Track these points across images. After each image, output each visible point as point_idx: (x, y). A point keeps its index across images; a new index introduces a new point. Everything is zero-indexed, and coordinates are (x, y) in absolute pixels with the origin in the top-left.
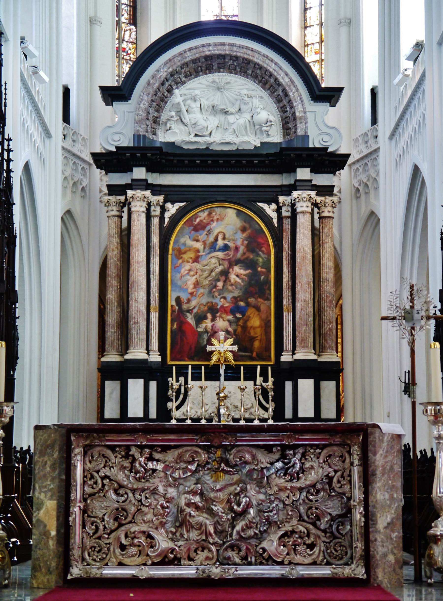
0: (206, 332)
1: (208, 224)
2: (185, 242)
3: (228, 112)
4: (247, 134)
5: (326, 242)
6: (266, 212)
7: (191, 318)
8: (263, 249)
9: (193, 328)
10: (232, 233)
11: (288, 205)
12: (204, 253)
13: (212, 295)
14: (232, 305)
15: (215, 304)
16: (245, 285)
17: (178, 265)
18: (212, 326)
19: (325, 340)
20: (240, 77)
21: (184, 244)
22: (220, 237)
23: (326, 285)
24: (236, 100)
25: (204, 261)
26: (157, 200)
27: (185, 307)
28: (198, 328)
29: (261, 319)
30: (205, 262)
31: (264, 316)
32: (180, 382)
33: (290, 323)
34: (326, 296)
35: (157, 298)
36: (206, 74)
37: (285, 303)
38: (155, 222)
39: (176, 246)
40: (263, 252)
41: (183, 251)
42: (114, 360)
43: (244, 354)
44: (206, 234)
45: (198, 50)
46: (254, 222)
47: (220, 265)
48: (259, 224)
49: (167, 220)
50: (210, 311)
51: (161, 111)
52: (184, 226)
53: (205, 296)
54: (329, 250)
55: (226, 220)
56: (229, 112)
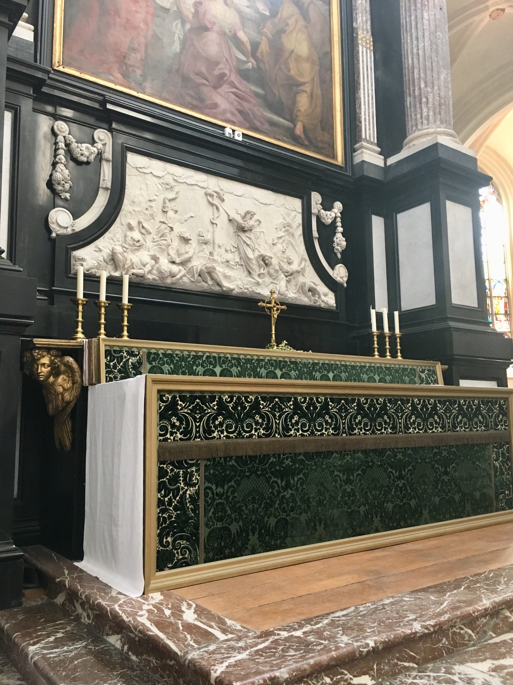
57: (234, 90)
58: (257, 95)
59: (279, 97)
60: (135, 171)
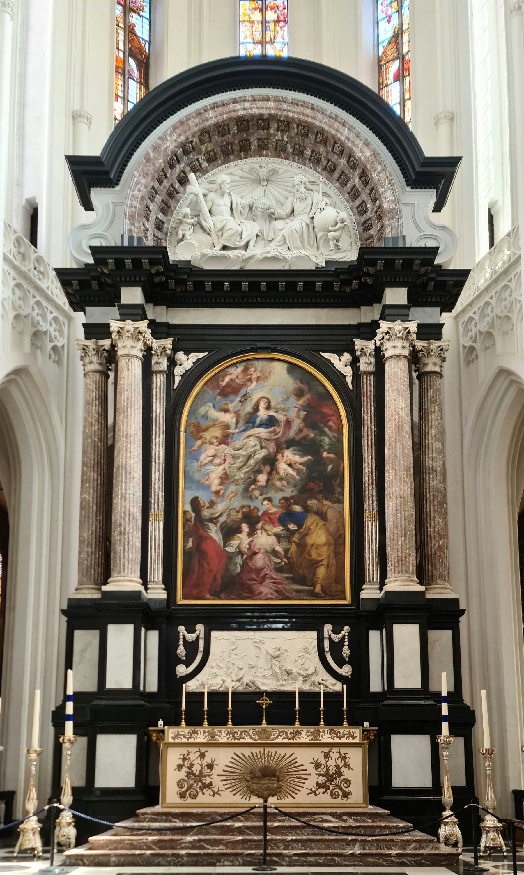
0: (240, 552)
1: (243, 385)
2: (207, 412)
3: (274, 214)
4: (304, 248)
5: (431, 411)
6: (335, 367)
7: (216, 532)
8: (331, 423)
9: (219, 546)
10: (280, 399)
11: (370, 355)
12: (237, 431)
13: (249, 495)
14: (281, 511)
15: (253, 509)
16: (302, 480)
17: (195, 448)
18: (250, 544)
19: (432, 565)
20: (292, 163)
21: (205, 416)
22: (262, 405)
23: (433, 478)
24: (287, 198)
25: (237, 442)
26: (162, 347)
27: (206, 513)
28: (227, 546)
29: (329, 533)
30: (237, 444)
31: (332, 528)
32: (197, 632)
33: (376, 538)
34: (433, 496)
35: (161, 500)
36: (240, 158)
37: (366, 506)
38: (159, 381)
39: (193, 420)
40: (330, 428)
41: (203, 427)
42: (89, 596)
43: (300, 587)
44: (240, 401)
45: (226, 109)
46: (316, 382)
47: (262, 448)
48: (323, 386)
49: (177, 379)
50: (246, 520)
51: (169, 213)
52: (205, 388)
53: (239, 495)
54: (437, 423)
55: (272, 380)
56: (276, 215)
57: (273, 581)
58: (287, 578)
59: (304, 575)
60: (215, 640)
